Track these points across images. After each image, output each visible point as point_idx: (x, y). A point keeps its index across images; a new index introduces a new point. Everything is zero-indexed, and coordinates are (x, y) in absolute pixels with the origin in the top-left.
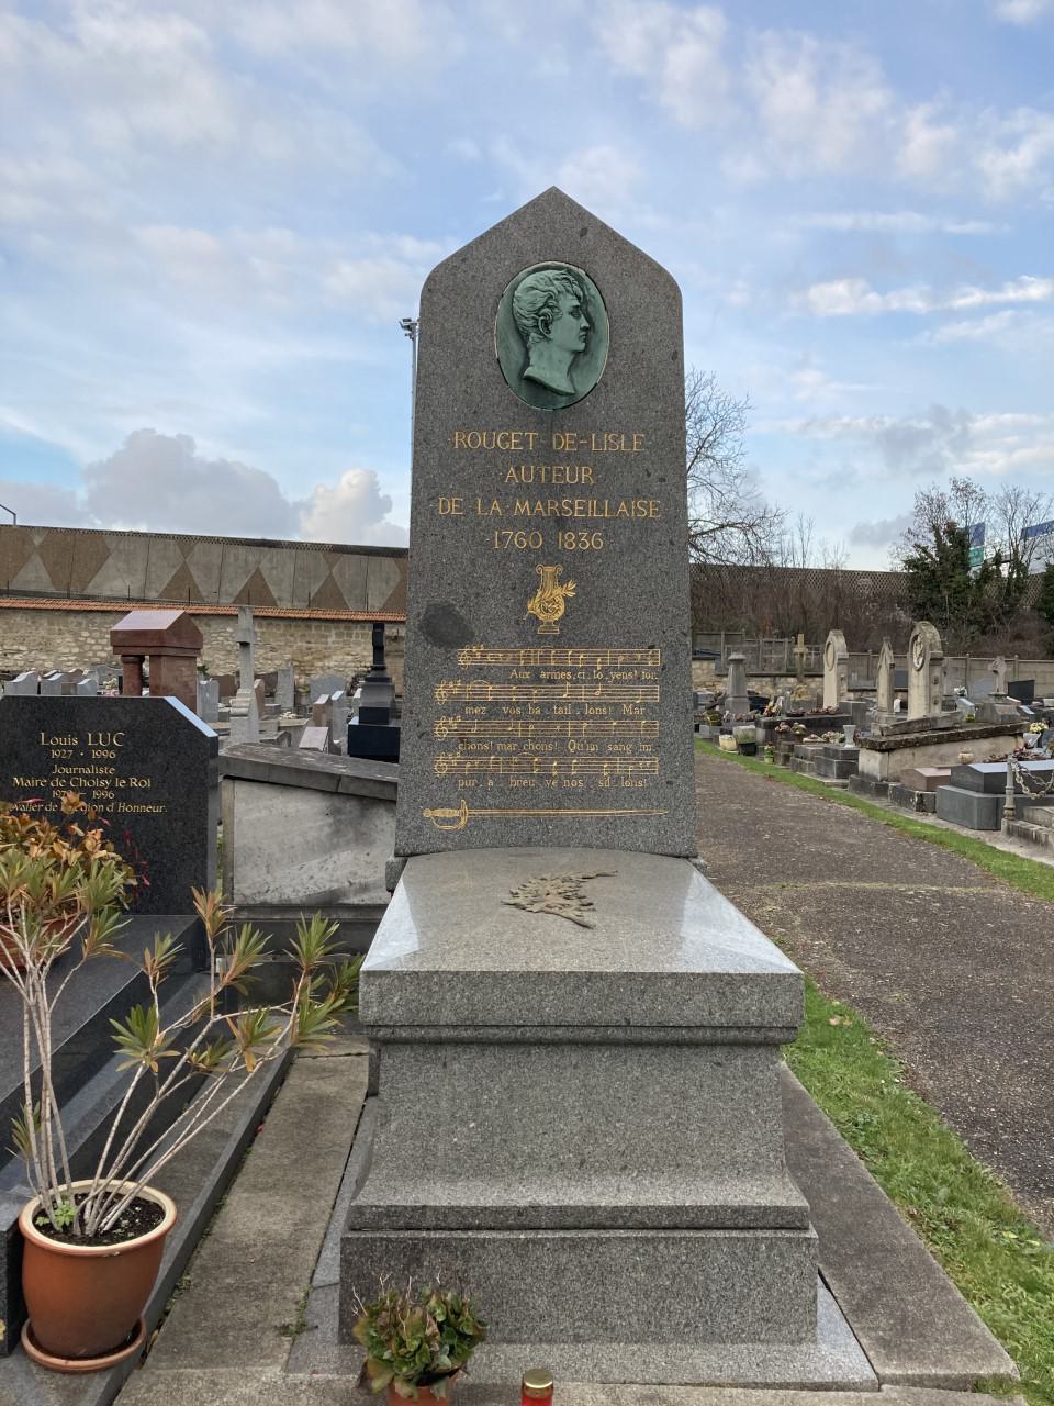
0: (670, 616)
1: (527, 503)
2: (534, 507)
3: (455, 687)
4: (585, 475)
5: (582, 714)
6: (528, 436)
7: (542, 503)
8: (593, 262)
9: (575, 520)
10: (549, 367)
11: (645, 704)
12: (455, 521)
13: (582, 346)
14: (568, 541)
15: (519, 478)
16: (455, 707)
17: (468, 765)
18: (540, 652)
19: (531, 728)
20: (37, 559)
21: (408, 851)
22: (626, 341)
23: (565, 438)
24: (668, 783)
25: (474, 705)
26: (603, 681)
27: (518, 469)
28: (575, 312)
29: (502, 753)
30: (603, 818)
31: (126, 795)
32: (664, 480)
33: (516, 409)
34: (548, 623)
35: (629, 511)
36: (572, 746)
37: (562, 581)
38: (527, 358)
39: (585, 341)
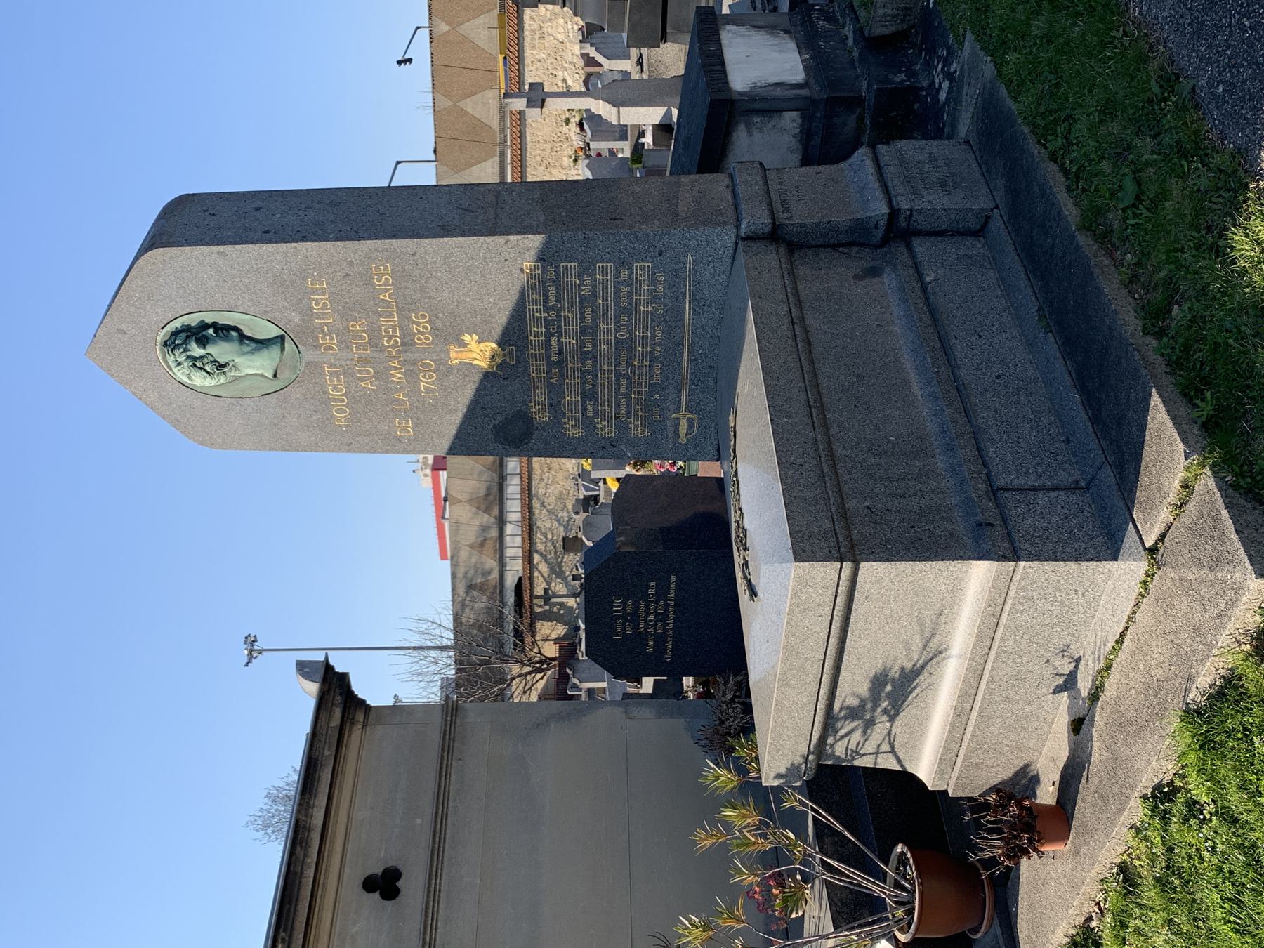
0: (488, 255)
3: (568, 424)
11: (580, 275)
16: (588, 423)
20: (465, 29)
25: (584, 409)
26: (558, 311)
27: (361, 380)
29: (629, 388)
30: (694, 310)
31: (661, 594)
35: (387, 290)
37: (463, 345)
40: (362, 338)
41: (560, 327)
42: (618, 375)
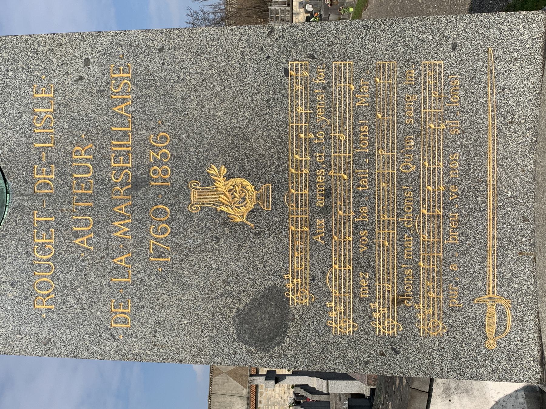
0: (248, 51)
1: (116, 224)
2: (121, 215)
4: (82, 156)
12: (138, 309)
14: (160, 174)
17: (432, 295)
18: (292, 207)
25: (357, 286)
27: (77, 235)
30: (499, 130)
32: (88, 59)
33: (8, 237)
35: (123, 101)
37: (209, 181)
41: (328, 155)
42: (402, 230)
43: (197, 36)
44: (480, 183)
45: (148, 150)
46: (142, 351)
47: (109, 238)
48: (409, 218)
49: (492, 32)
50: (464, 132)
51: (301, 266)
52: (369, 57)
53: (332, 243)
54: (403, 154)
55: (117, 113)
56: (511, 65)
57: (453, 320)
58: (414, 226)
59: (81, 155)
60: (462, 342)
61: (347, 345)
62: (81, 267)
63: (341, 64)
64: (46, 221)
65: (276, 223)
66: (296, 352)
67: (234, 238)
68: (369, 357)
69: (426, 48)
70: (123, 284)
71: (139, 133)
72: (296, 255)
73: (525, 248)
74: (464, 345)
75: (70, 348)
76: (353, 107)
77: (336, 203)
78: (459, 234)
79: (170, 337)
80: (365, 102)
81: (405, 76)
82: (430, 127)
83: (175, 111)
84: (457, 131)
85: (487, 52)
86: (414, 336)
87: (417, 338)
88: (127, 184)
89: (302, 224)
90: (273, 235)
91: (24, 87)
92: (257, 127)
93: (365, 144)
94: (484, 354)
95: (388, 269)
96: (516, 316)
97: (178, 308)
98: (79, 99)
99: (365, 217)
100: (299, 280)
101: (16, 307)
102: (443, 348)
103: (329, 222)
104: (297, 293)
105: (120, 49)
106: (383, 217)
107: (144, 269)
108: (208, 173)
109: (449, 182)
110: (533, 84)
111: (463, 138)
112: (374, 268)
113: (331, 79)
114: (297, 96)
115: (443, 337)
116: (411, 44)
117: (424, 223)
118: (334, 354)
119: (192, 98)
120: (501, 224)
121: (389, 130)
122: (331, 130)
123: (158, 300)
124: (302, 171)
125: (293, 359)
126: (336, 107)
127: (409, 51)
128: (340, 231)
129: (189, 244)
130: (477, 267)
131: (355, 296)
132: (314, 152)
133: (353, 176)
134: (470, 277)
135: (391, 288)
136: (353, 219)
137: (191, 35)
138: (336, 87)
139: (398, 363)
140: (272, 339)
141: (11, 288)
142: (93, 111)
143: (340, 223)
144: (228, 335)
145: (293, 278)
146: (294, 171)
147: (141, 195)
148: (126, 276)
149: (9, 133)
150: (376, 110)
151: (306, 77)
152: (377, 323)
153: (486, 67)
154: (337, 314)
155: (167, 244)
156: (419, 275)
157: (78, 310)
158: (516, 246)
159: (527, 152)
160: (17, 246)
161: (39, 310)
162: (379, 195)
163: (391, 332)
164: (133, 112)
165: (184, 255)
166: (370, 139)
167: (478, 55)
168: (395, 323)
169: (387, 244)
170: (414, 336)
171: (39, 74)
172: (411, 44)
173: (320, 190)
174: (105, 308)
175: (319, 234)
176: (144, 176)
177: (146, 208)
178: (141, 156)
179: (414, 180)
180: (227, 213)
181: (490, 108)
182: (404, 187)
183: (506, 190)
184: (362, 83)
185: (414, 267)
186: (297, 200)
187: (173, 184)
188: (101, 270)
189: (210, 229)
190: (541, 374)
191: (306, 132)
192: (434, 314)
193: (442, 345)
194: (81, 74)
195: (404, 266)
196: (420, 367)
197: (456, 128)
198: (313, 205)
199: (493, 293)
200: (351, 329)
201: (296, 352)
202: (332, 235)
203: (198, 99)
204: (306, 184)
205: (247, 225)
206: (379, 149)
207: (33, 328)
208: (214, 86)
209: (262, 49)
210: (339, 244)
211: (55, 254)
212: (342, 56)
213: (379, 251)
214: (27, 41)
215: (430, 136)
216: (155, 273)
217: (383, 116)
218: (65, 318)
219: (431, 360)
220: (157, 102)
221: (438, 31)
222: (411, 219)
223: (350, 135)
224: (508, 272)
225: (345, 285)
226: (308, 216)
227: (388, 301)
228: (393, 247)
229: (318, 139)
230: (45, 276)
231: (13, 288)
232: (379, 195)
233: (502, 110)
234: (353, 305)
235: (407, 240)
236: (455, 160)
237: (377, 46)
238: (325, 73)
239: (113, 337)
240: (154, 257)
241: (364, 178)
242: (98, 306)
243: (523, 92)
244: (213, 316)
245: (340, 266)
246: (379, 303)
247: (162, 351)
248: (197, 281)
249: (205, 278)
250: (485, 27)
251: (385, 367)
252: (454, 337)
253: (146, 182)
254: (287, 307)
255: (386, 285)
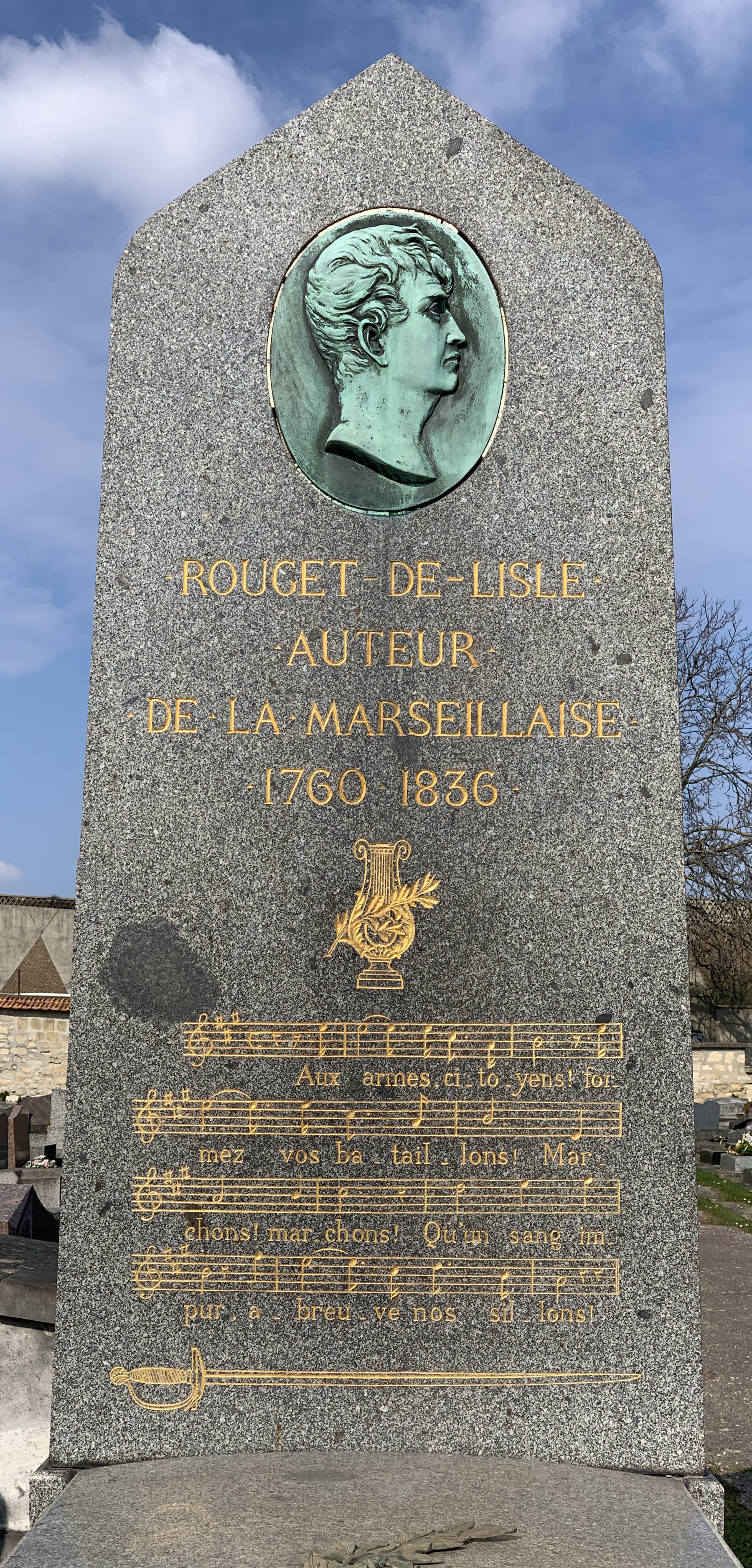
0: (642, 949)
1: (334, 708)
2: (349, 717)
4: (457, 648)
5: (454, 1164)
6: (338, 566)
7: (367, 708)
8: (471, 208)
9: (435, 745)
10: (378, 418)
12: (181, 747)
13: (449, 381)
14: (422, 788)
15: (317, 655)
17: (205, 1274)
18: (363, 1028)
19: (343, 1194)
21: (77, 1457)
22: (542, 369)
23: (415, 571)
24: (640, 1314)
25: (219, 1143)
26: (500, 1092)
27: (314, 637)
28: (437, 308)
29: (279, 1247)
32: (629, 661)
33: (311, 513)
34: (378, 966)
35: (555, 724)
36: (431, 1234)
37: (409, 876)
38: (335, 406)
39: (456, 369)
40: (431, 656)
41: (457, 1094)
42: (320, 1224)
43: (669, 858)
44: (404, 1359)
45: (466, 767)
46: (105, 754)
47: (307, 695)
48: (342, 1236)
49: (669, 1379)
50: (494, 1330)
51: (255, 1044)
52: (629, 1166)
53: (296, 1099)
54: (456, 1226)
55: (532, 711)
56: (610, 1413)
57: (160, 1310)
58: (327, 1245)
59: (458, 646)
60: (123, 1327)
61: (114, 1124)
62: (255, 644)
63: (618, 1116)
64: (339, 582)
65: (334, 998)
66: (101, 1032)
67: (306, 920)
68: (94, 1162)
69: (643, 1265)
70: (225, 719)
71: (498, 752)
72: (275, 1034)
73: (289, 1435)
74: (117, 1328)
75: (111, 623)
76: (541, 1139)
77: (370, 1107)
78: (313, 1322)
79: (129, 804)
80: (549, 1160)
81: (594, 1229)
82: (502, 1272)
83: (537, 816)
84: (495, 1318)
85: (634, 1372)
86: (132, 1243)
87: (129, 1248)
88: (405, 729)
89: (330, 1045)
90: (311, 991)
91: (581, 545)
92: (508, 965)
93: (475, 1159)
94: (100, 1365)
95: (249, 1199)
96: (169, 1420)
97: (181, 818)
98: (558, 644)
99: (344, 1160)
100: (228, 1040)
101: (185, 526)
102: (112, 1293)
103: (334, 1094)
104: (206, 1035)
105: (647, 718)
106: (344, 1192)
107: (251, 757)
108: (424, 875)
109: (405, 1305)
110: (577, 1450)
111: (483, 1330)
112: (252, 1174)
113: (592, 1099)
114: (563, 1037)
115: (132, 1292)
116: (650, 1239)
117: (332, 1262)
118: (99, 1100)
119: (560, 847)
120: (330, 1395)
121: (499, 1202)
122: (501, 1099)
123: (196, 783)
124: (428, 1047)
125: (89, 1027)
126: (541, 1107)
127: (637, 1235)
128: (318, 1114)
129: (296, 839)
130: (256, 1353)
131: (201, 1140)
132: (463, 1069)
133: (418, 1138)
134: (238, 1340)
135: (217, 1199)
136: (339, 1138)
137: (671, 846)
138: (578, 1107)
139: (83, 1213)
140: (123, 990)
141: (220, 518)
142: (537, 668)
143: (333, 1114)
144: (131, 909)
145: (233, 1028)
146: (428, 1031)
147: (384, 753)
148: (240, 726)
149: (497, 516)
150: (535, 1178)
151: (596, 1054)
152: (154, 1178)
153: (608, 1370)
154: (168, 1106)
155: (296, 800)
156: (240, 1254)
157: (179, 638)
158: (292, 1419)
159: (458, 1439)
160: (295, 529)
161: (180, 569)
162: (382, 1184)
163: (139, 1202)
164: (535, 740)
165: (276, 829)
166: (483, 1168)
167: (628, 1356)
168: (155, 1210)
169: (296, 1197)
170: (132, 1243)
171: (603, 571)
172: (650, 1239)
173: (392, 1078)
174: (182, 686)
175: (314, 1077)
176: (420, 758)
177: (361, 761)
178: (456, 755)
179: (409, 1246)
180: (351, 909)
181: (535, 1376)
182: (396, 1228)
183: (390, 1403)
184: (583, 1154)
185: (255, 1244)
186: (374, 1036)
187: (405, 811)
188: (251, 681)
189: (322, 878)
190: (66, 1462)
191: (499, 1053)
192: (171, 1277)
193: (116, 1290)
194: (603, 648)
195: (256, 1227)
196: (77, 1252)
197: (502, 1318)
198: (365, 1065)
199: (210, 1380)
200: (143, 1132)
201: (101, 1032)
202: (310, 1099)
203: (557, 858)
204: (404, 1053)
205: (330, 944)
206: (466, 1183)
207: (148, 557)
208: (581, 887)
209: (646, 974)
210: (294, 1112)
211: (280, 597)
212: (631, 1118)
213: (281, 1183)
214: (662, 551)
215: (488, 1272)
216: (244, 777)
217: (525, 1191)
218: (164, 615)
219: (90, 1272)
220: (553, 785)
221: (672, 1287)
222: (340, 1240)
223: (491, 1132)
224: (247, 1405)
225: (221, 1121)
226: (345, 1056)
227: (193, 1198)
228: (289, 1208)
229: (485, 1076)
230: (240, 579)
231: (220, 522)
232: (382, 1184)
233: (531, 1396)
234: (185, 1137)
235: (301, 1234)
236: (445, 1316)
237: (648, 1179)
238: (602, 1088)
239: (131, 702)
240: (272, 776)
241: (415, 1158)
242: (186, 675)
243: (562, 1433)
244: (167, 882)
245: (254, 1113)
246: (189, 1182)
247: (105, 790)
248: (230, 854)
249: (234, 867)
250: (677, 1368)
251: (76, 1191)
252: (130, 1312)
253: (409, 762)
254: (181, 1018)
255: (222, 1195)
